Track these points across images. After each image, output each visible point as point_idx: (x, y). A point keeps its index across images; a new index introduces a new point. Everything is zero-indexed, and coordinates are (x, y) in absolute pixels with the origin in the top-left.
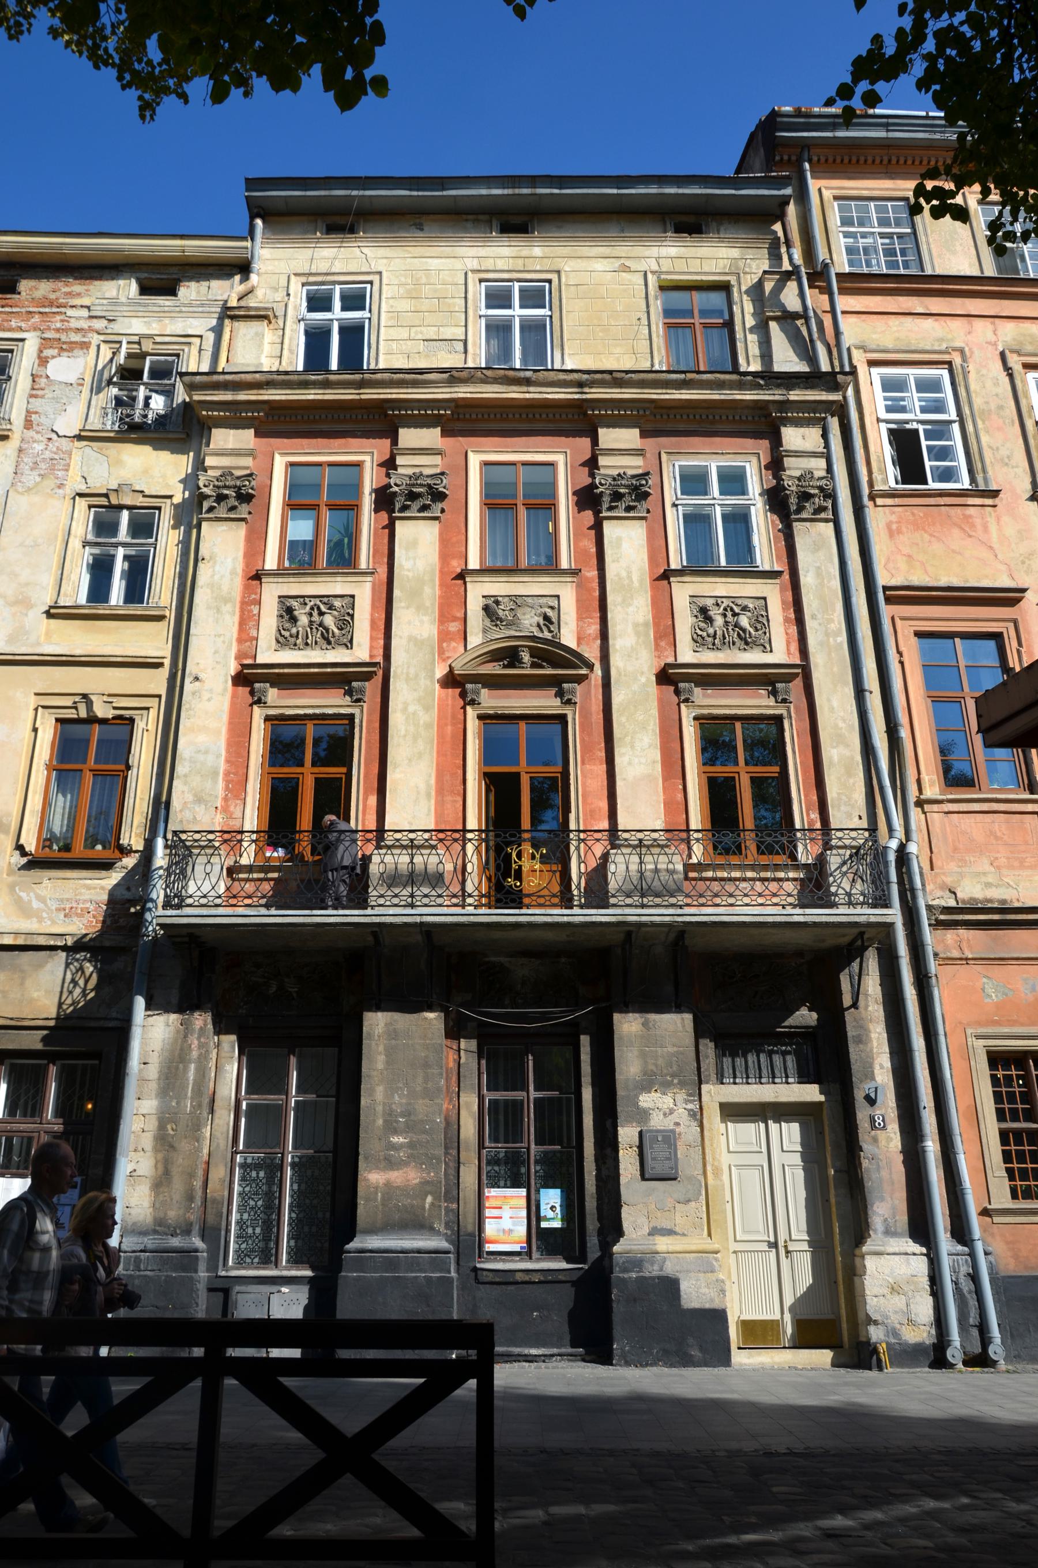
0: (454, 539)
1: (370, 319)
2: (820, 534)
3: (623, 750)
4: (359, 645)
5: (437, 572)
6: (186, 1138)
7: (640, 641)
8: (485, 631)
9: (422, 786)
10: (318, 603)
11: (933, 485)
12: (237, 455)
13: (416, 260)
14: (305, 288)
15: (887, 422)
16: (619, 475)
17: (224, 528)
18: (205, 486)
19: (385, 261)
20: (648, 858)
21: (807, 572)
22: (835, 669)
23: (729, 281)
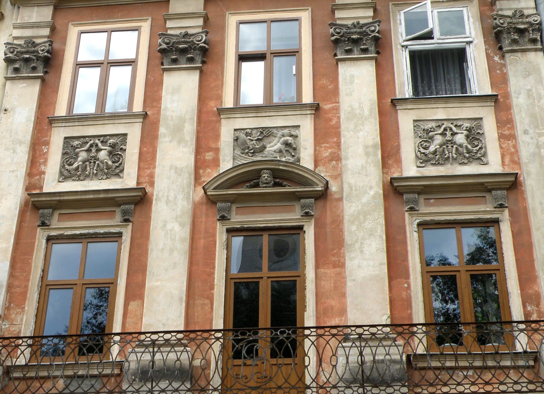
3: (353, 255)
4: (129, 174)
7: (369, 160)
8: (234, 159)
10: (97, 141)
16: (353, 24)
18: (12, 53)
20: (367, 351)
21: (519, 94)
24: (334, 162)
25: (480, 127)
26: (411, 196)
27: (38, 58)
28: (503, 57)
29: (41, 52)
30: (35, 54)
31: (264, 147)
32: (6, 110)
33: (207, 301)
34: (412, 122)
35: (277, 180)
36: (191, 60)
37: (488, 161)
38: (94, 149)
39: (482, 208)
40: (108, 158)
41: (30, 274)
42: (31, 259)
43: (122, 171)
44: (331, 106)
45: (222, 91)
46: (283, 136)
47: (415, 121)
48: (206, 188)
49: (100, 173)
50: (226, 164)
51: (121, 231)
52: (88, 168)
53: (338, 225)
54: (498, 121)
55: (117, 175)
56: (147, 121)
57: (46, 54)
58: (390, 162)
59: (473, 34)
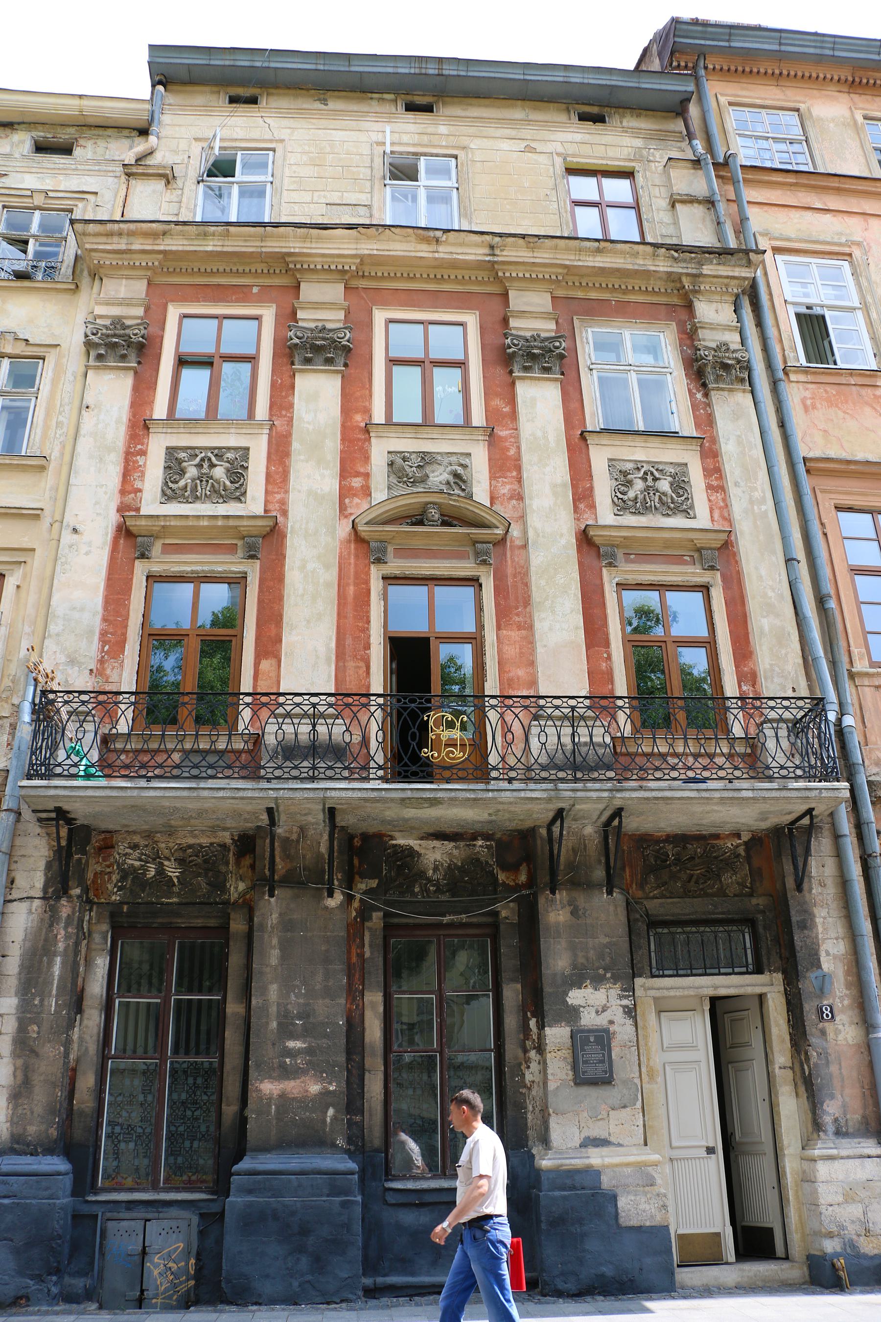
0: (358, 394)
1: (272, 183)
2: (738, 404)
3: (543, 615)
4: (253, 499)
5: (339, 426)
6: (49, 1042)
9: (322, 650)
10: (209, 454)
11: (840, 365)
12: (128, 305)
13: (320, 131)
15: (794, 304)
16: (533, 336)
17: (112, 376)
18: (93, 334)
19: (289, 131)
21: (728, 440)
22: (761, 537)
23: (634, 167)
24: (514, 502)
25: (685, 474)
27: (130, 344)
28: (706, 395)
30: (126, 338)
32: (87, 407)
33: (362, 664)
35: (446, 518)
36: (329, 361)
37: (695, 514)
38: (206, 465)
39: (690, 569)
40: (225, 476)
41: (127, 619)
42: (129, 599)
44: (507, 432)
45: (370, 403)
47: (610, 460)
48: (357, 521)
52: (199, 488)
54: (704, 469)
55: (238, 499)
57: (141, 339)
58: (582, 506)
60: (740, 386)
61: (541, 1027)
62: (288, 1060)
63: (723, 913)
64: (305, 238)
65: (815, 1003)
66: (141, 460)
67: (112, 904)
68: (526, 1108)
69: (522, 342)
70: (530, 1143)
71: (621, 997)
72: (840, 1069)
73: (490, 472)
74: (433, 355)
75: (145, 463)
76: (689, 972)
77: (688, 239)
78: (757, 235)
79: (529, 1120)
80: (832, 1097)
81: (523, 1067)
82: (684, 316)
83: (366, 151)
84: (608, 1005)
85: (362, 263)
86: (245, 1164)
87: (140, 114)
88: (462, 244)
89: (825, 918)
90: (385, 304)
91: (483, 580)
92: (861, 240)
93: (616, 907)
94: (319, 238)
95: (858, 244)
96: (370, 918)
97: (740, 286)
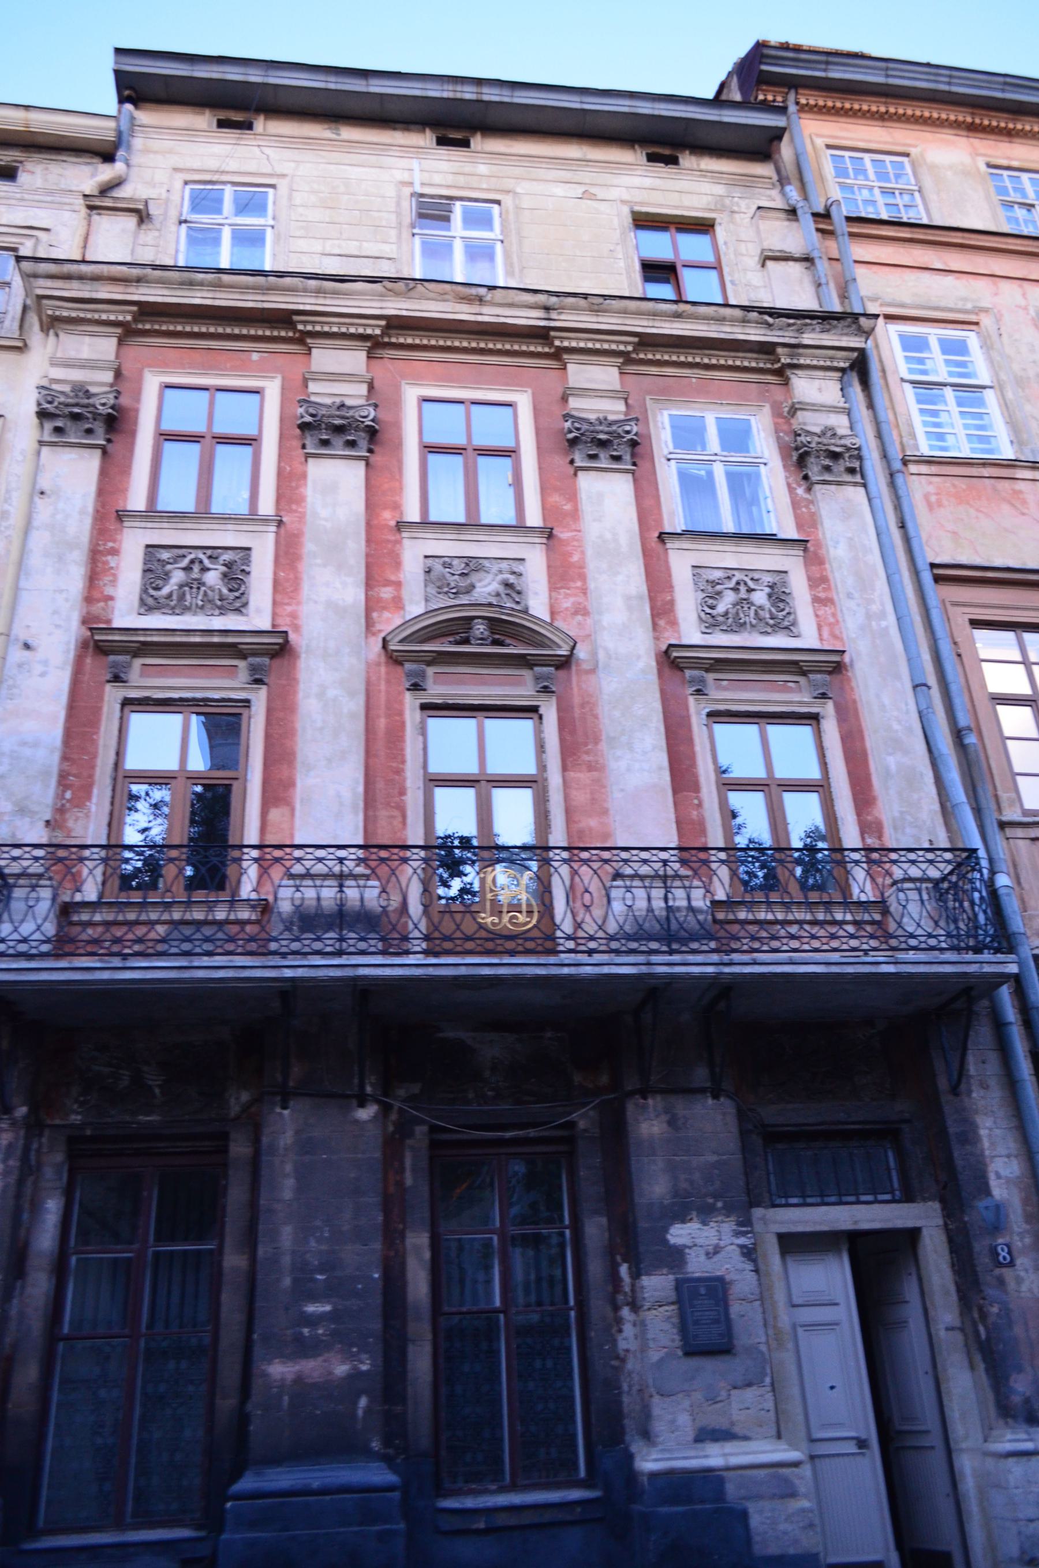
0: (386, 486)
3: (619, 753)
4: (258, 611)
8: (427, 600)
9: (347, 795)
10: (201, 556)
12: (92, 368)
13: (332, 167)
14: (188, 187)
16: (598, 419)
18: (50, 403)
19: (293, 165)
21: (837, 542)
23: (714, 220)
24: (579, 618)
25: (784, 584)
26: (696, 673)
27: (96, 416)
28: (809, 490)
29: (101, 408)
30: (91, 409)
31: (473, 587)
33: (396, 813)
34: (690, 568)
35: (497, 636)
36: (352, 444)
38: (196, 568)
39: (796, 697)
40: (220, 582)
42: (97, 733)
43: (245, 605)
46: (500, 572)
48: (388, 638)
49: (209, 606)
50: (415, 607)
51: (249, 697)
52: (188, 597)
53: (591, 710)
54: (809, 579)
55: (238, 611)
56: (282, 530)
57: (110, 411)
58: (662, 623)
59: (766, 454)
60: (848, 478)
61: (636, 1275)
62: (306, 1331)
63: (859, 1123)
64: (319, 291)
65: (986, 1242)
66: (112, 561)
67: (72, 1126)
68: (619, 1388)
69: (585, 427)
70: (627, 1438)
71: (738, 1234)
72: (1027, 1331)
73: (549, 582)
74: (479, 441)
75: (118, 564)
76: (818, 1200)
77: (782, 302)
78: (865, 300)
79: (625, 1405)
80: (1020, 1370)
81: (614, 1329)
82: (778, 393)
83: (391, 191)
84: (722, 1243)
85: (388, 327)
86: (246, 1483)
87: (103, 131)
88: (511, 305)
89: (990, 1129)
90: (417, 379)
91: (542, 711)
92: (990, 306)
93: (724, 1114)
94: (335, 292)
95: (986, 310)
96: (411, 1134)
97: (846, 359)
